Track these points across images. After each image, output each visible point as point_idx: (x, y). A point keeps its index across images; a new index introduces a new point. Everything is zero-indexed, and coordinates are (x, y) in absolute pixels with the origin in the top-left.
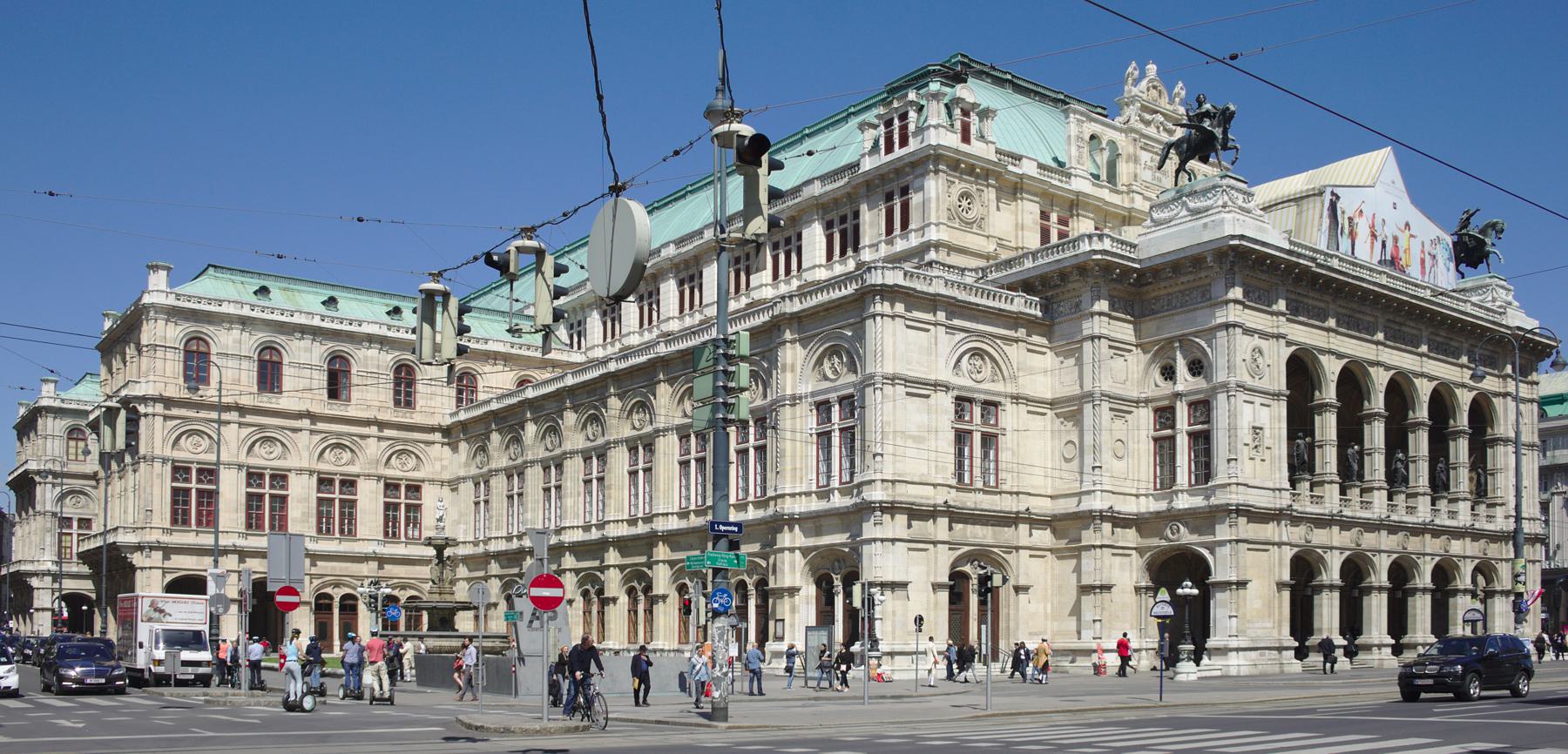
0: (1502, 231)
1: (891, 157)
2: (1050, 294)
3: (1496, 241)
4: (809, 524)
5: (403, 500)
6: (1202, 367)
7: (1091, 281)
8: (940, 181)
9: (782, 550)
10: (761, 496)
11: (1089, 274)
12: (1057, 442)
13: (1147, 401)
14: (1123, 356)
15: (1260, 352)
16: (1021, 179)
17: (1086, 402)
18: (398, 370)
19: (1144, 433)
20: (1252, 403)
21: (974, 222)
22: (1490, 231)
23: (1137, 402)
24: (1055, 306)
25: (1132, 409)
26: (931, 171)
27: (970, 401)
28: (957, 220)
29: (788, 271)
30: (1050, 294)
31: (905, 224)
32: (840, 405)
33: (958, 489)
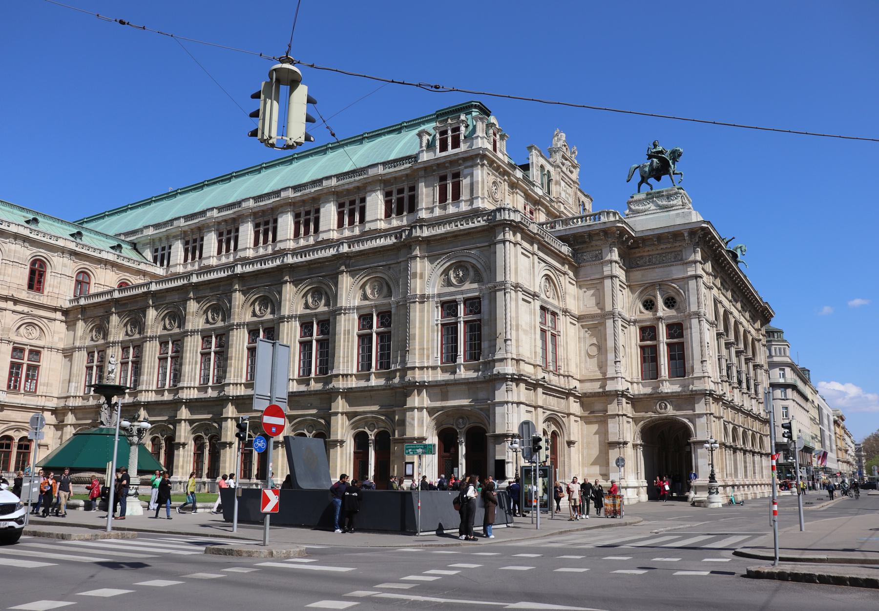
1: (444, 154)
2: (577, 247)
4: (437, 390)
5: (25, 361)
6: (675, 302)
7: (610, 240)
9: (412, 409)
10: (204, 384)
11: (609, 236)
12: (582, 345)
13: (635, 322)
17: (609, 318)
18: (33, 263)
19: (633, 342)
24: (579, 255)
26: (478, 164)
29: (228, 250)
30: (577, 247)
32: (465, 304)
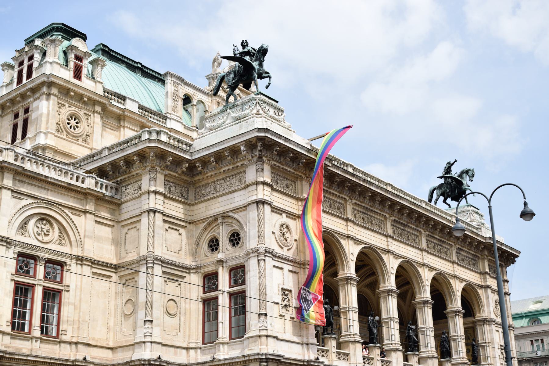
0: (473, 176)
2: (119, 179)
3: (469, 183)
6: (239, 239)
7: (149, 164)
8: (51, 102)
13: (197, 268)
14: (178, 230)
15: (287, 227)
16: (124, 112)
20: (282, 269)
21: (81, 136)
22: (464, 175)
23: (188, 269)
24: (124, 189)
25: (185, 275)
26: (44, 93)
27: (35, 258)
28: (65, 133)
30: (119, 179)
31: (24, 135)
33: (13, 337)
